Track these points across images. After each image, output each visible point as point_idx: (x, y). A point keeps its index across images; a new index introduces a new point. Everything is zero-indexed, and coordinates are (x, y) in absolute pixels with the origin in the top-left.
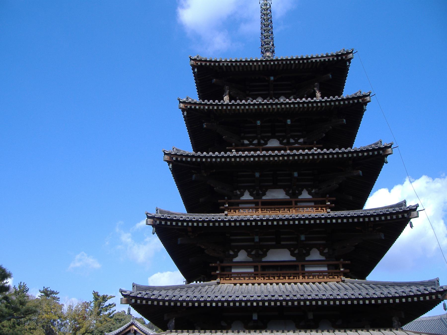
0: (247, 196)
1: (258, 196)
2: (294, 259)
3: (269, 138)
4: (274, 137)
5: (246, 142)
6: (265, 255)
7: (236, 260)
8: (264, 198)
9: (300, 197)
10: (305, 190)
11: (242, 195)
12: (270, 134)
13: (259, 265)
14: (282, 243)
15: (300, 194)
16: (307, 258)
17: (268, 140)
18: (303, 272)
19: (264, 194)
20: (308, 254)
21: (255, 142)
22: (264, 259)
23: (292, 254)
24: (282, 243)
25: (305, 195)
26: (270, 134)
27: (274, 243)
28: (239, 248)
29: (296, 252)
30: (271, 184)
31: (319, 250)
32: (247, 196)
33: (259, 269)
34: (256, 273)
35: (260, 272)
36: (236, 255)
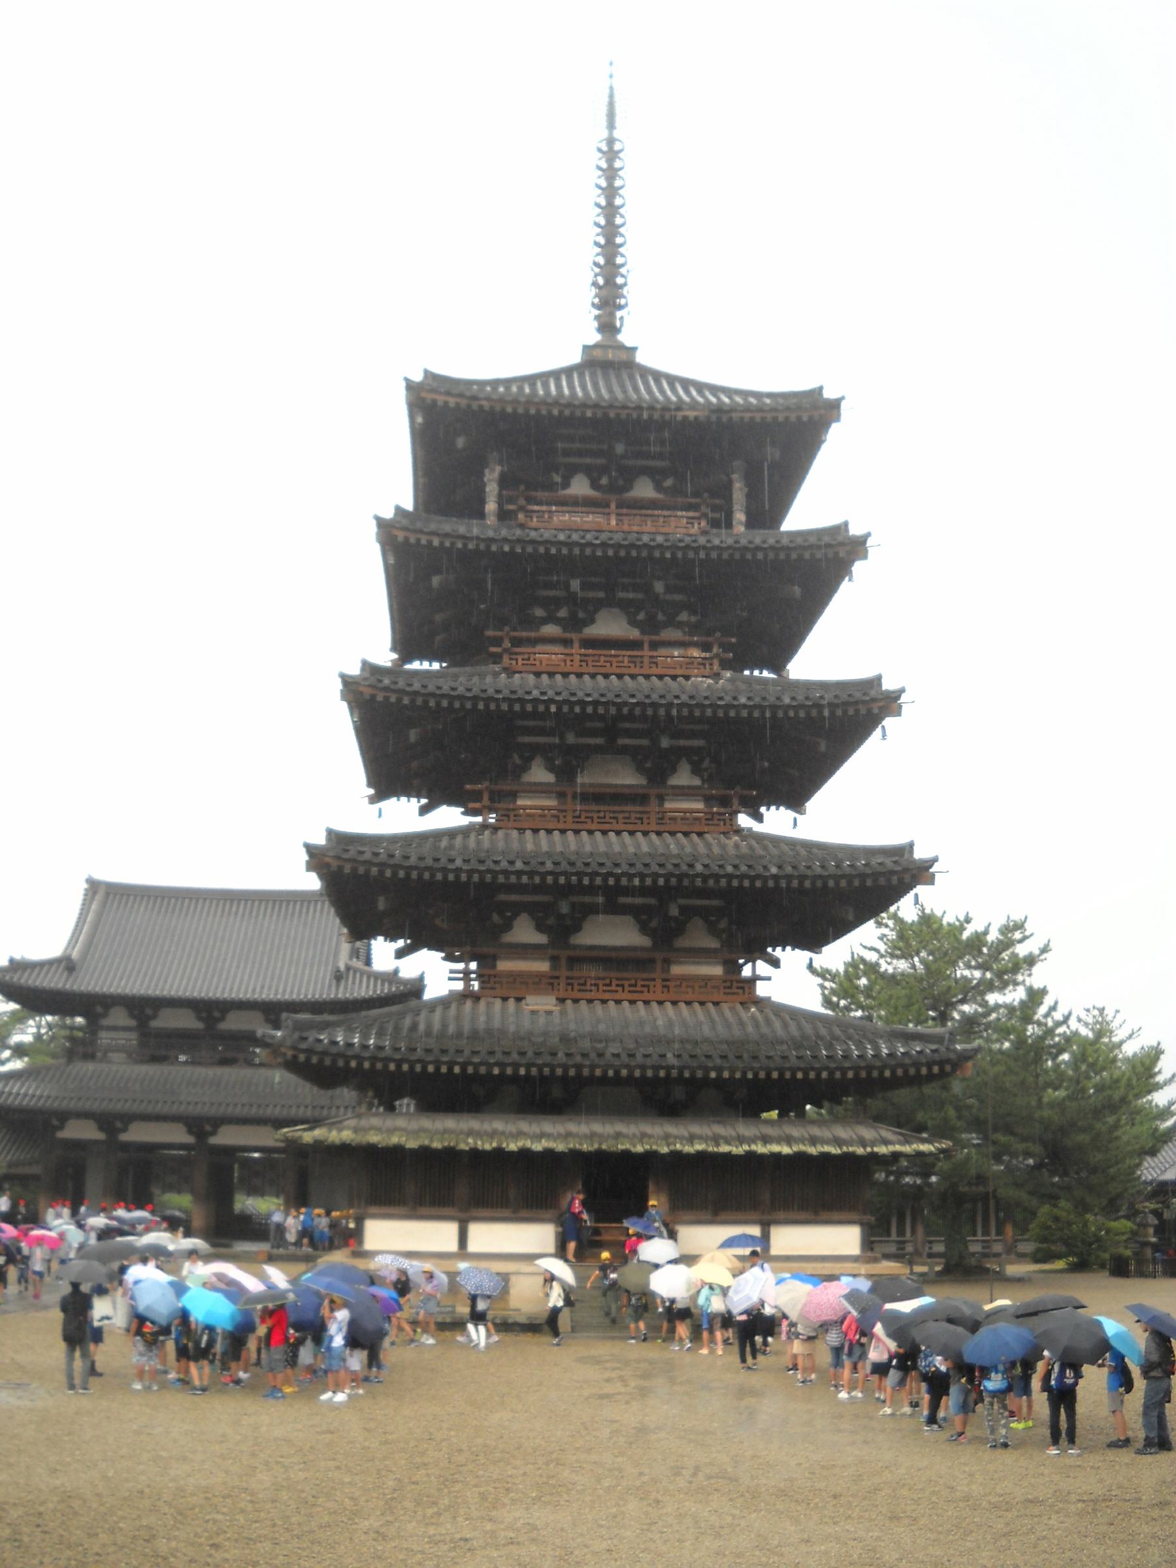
1: (566, 773)
3: (599, 605)
4: (610, 602)
5: (539, 612)
6: (577, 928)
10: (684, 759)
12: (601, 595)
13: (564, 954)
14: (623, 900)
17: (596, 610)
18: (664, 976)
21: (563, 613)
23: (644, 929)
24: (623, 900)
26: (601, 595)
28: (518, 909)
29: (654, 924)
33: (563, 962)
34: (556, 974)
35: (564, 972)
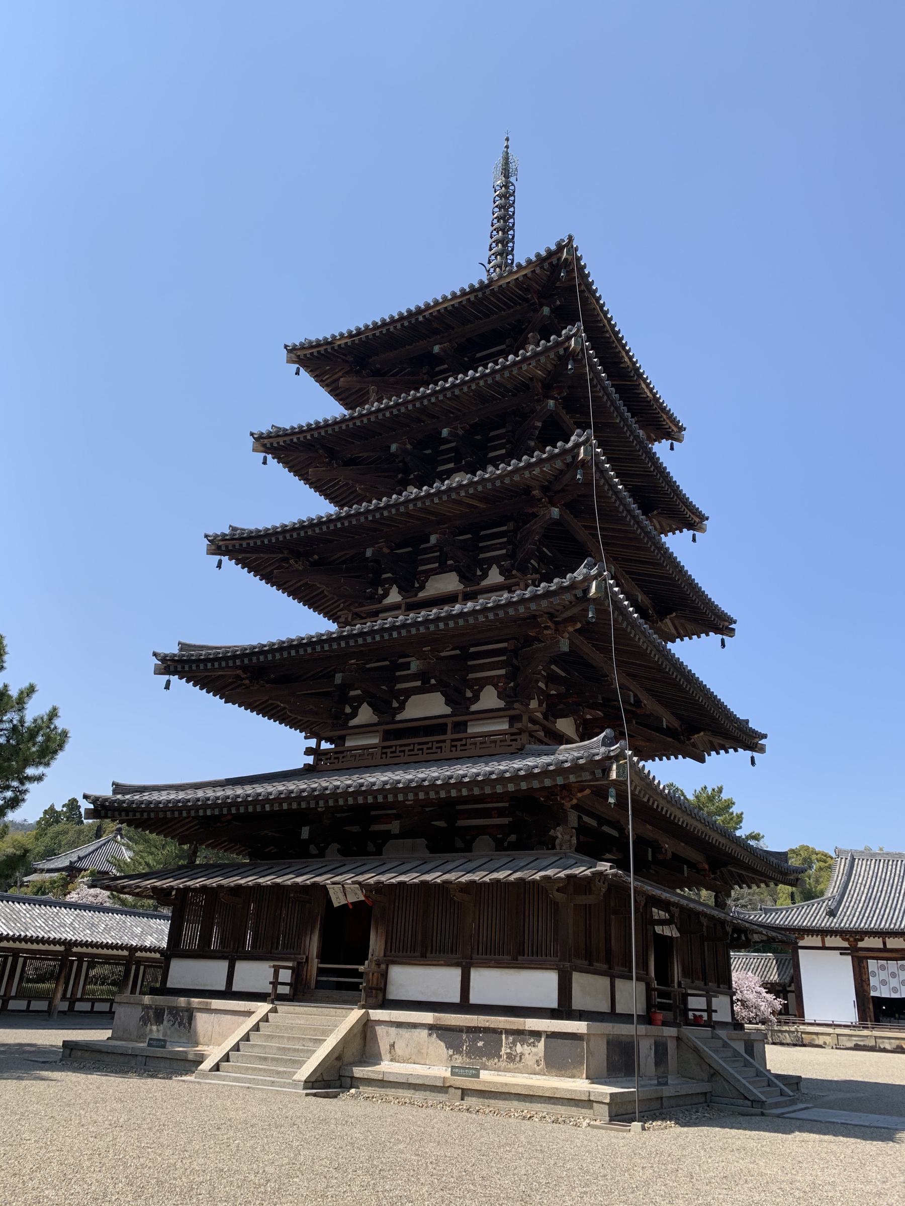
0: (394, 597)
2: (448, 710)
6: (402, 707)
7: (353, 723)
8: (421, 595)
9: (484, 583)
10: (494, 566)
11: (386, 595)
12: (452, 465)
15: (485, 575)
16: (474, 708)
19: (422, 588)
20: (476, 698)
22: (399, 717)
25: (495, 577)
26: (452, 465)
27: (419, 683)
30: (437, 565)
31: (496, 686)
32: (394, 597)
36: (354, 715)
